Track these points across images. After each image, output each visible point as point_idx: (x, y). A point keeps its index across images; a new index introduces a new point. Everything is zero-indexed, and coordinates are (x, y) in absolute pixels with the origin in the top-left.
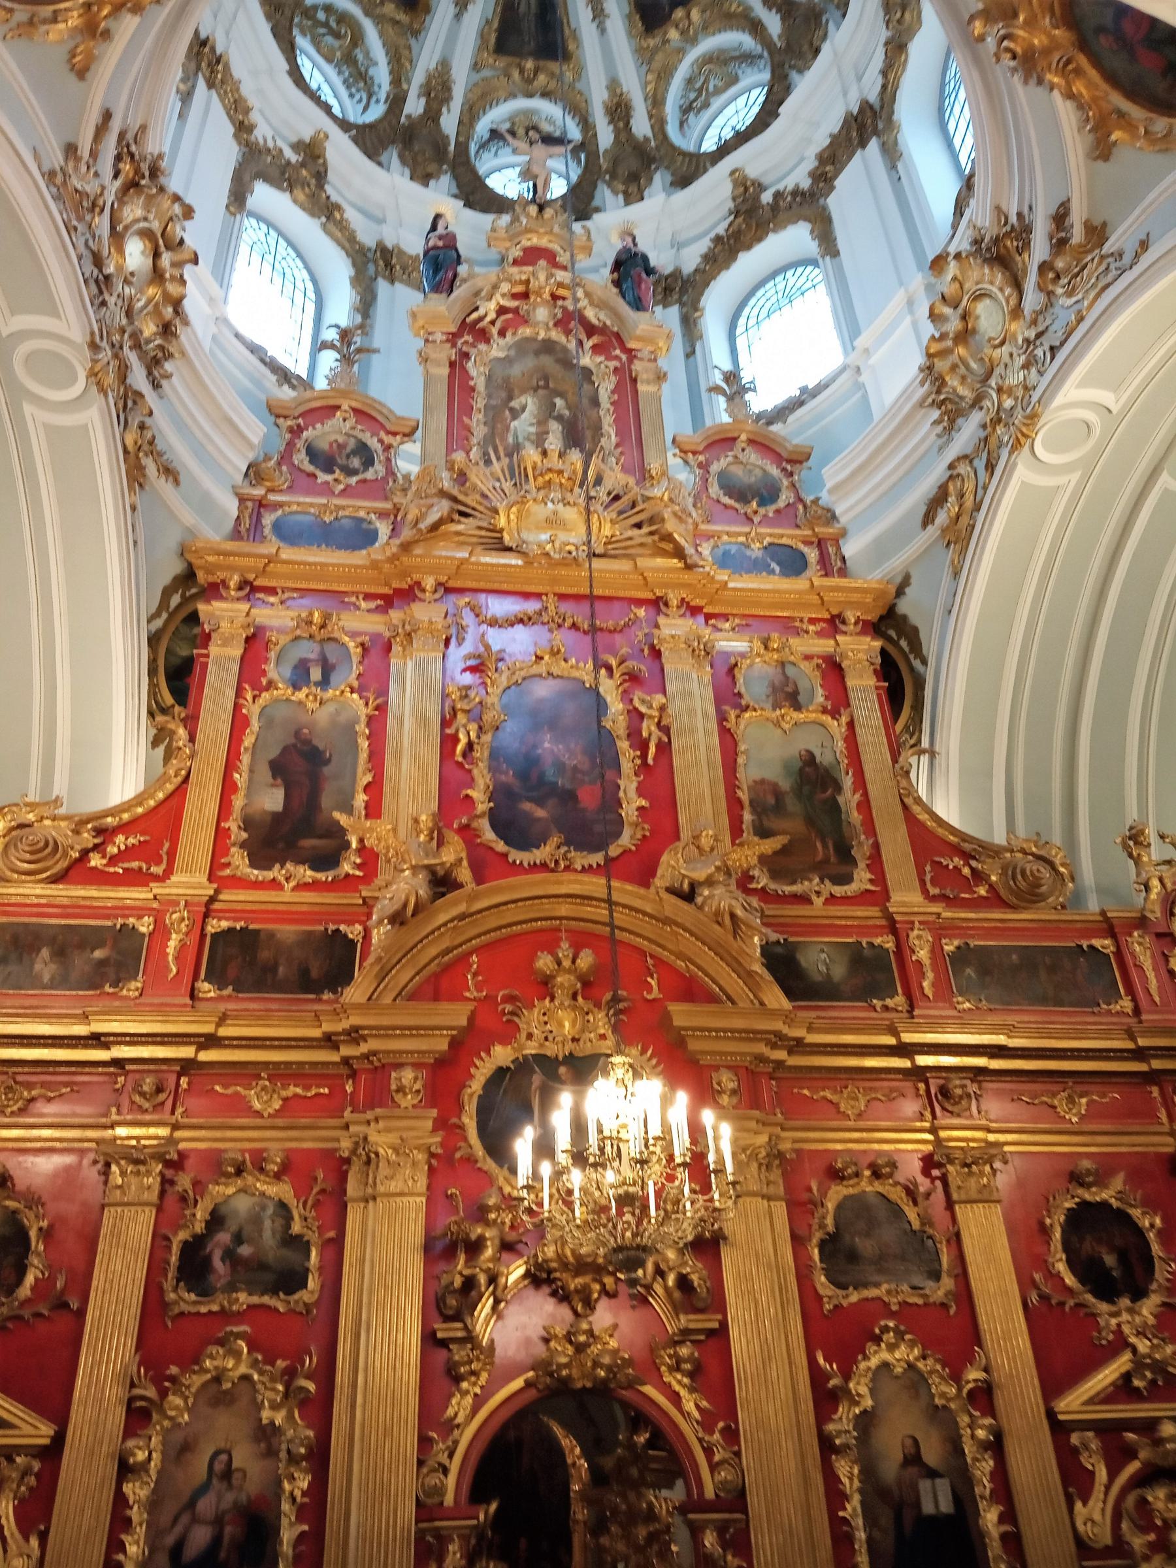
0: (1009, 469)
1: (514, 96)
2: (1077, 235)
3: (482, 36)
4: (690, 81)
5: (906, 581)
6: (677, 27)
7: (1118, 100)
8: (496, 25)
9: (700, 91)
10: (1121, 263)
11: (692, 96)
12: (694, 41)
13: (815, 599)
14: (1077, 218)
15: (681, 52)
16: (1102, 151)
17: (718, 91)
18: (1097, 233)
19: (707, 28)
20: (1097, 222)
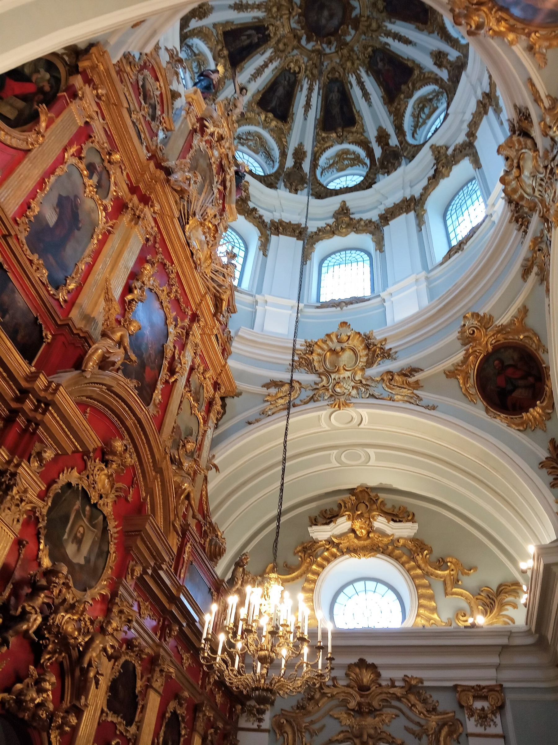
0: (321, 408)
1: (211, 51)
2: (412, 380)
3: (227, 23)
4: (249, 133)
5: (239, 394)
6: (266, 117)
7: (473, 373)
8: (233, 27)
9: (247, 139)
10: (415, 400)
11: (244, 137)
12: (264, 128)
13: (219, 370)
14: (418, 376)
15: (258, 124)
16: (451, 374)
17: (249, 147)
18: (417, 385)
19: (271, 131)
20: (421, 384)
